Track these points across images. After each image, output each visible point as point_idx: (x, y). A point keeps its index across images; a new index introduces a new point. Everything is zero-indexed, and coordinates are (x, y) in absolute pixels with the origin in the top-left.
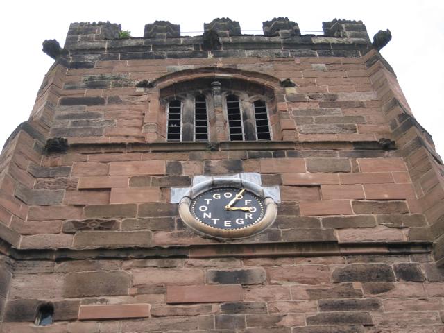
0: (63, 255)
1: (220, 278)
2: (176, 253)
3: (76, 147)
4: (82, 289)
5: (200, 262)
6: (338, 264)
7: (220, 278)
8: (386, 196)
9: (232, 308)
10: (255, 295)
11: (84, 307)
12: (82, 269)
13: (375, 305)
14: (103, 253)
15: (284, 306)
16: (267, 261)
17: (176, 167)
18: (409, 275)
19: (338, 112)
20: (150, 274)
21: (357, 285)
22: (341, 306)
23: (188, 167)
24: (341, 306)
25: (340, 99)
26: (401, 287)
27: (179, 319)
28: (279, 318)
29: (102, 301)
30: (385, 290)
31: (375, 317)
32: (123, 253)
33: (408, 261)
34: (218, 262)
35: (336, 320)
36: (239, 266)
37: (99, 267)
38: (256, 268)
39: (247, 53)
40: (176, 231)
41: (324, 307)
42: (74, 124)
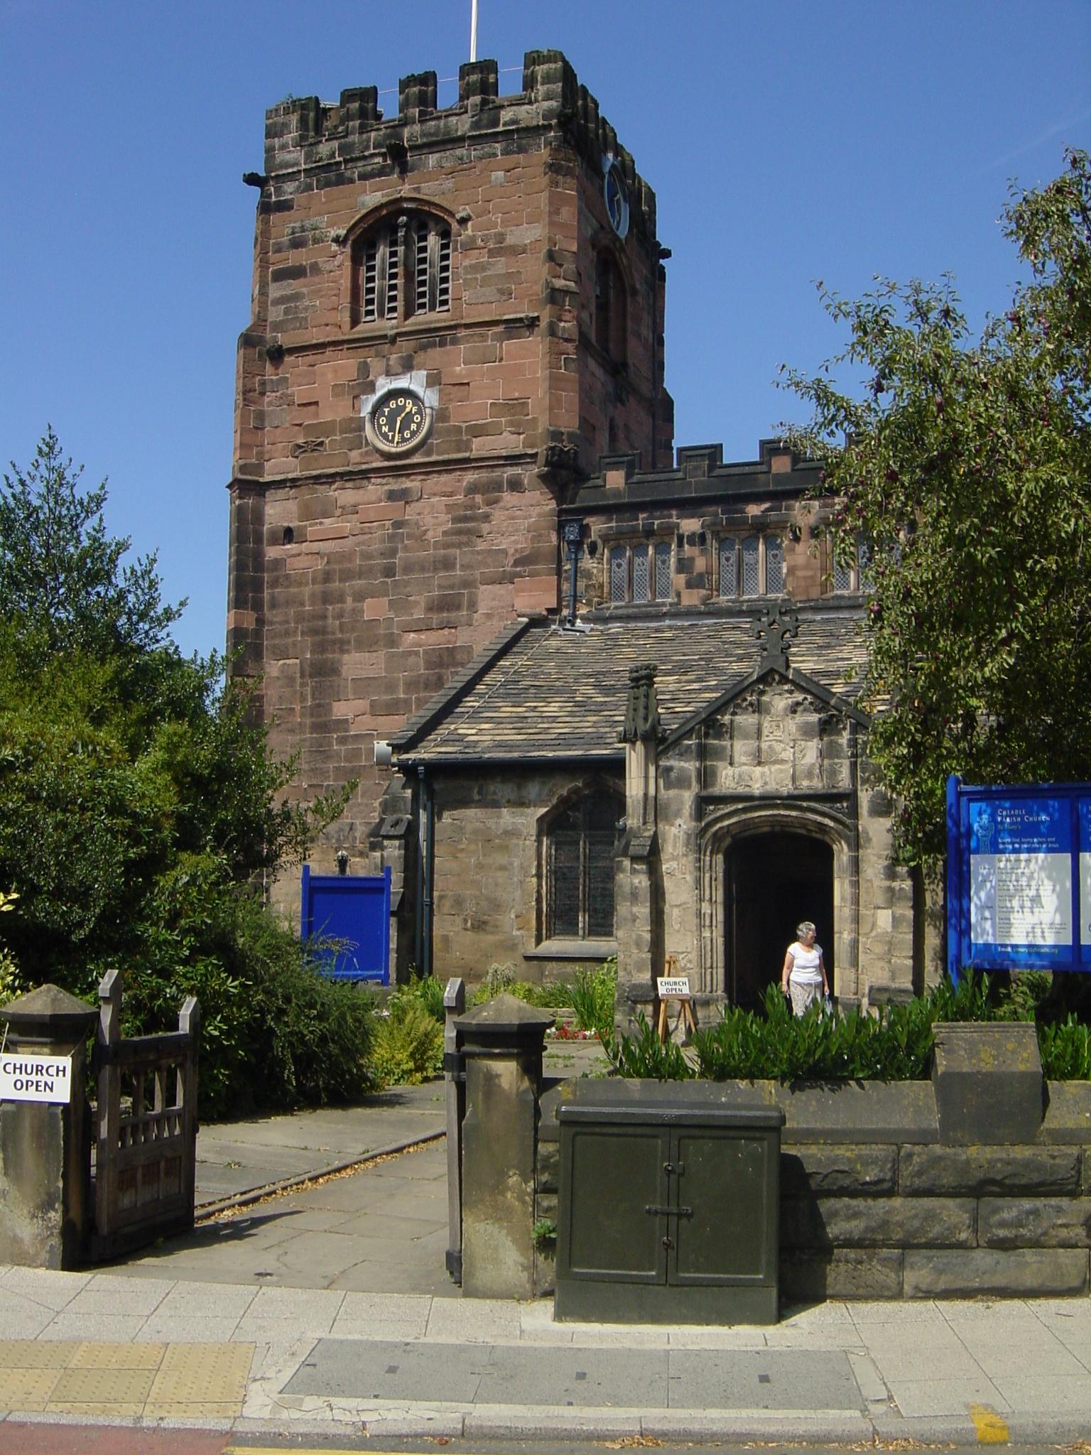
0: (294, 483)
1: (392, 496)
2: (364, 475)
3: (292, 351)
4: (308, 514)
5: (379, 480)
6: (470, 477)
7: (392, 496)
8: (516, 395)
9: (398, 525)
10: (411, 513)
11: (312, 530)
12: (306, 494)
13: (486, 518)
14: (317, 479)
15: (428, 520)
16: (422, 477)
17: (364, 369)
18: (515, 485)
19: (501, 265)
20: (345, 495)
21: (478, 498)
22: (465, 519)
23: (376, 364)
24: (465, 519)
25: (510, 240)
26: (508, 498)
27: (367, 537)
28: (426, 531)
29: (321, 523)
30: (496, 501)
31: (485, 528)
32: (331, 478)
33: (518, 470)
34: (391, 480)
35: (459, 532)
36: (406, 484)
37: (316, 491)
38: (412, 484)
39: (432, 160)
40: (364, 449)
41: (455, 520)
42: (286, 312)
